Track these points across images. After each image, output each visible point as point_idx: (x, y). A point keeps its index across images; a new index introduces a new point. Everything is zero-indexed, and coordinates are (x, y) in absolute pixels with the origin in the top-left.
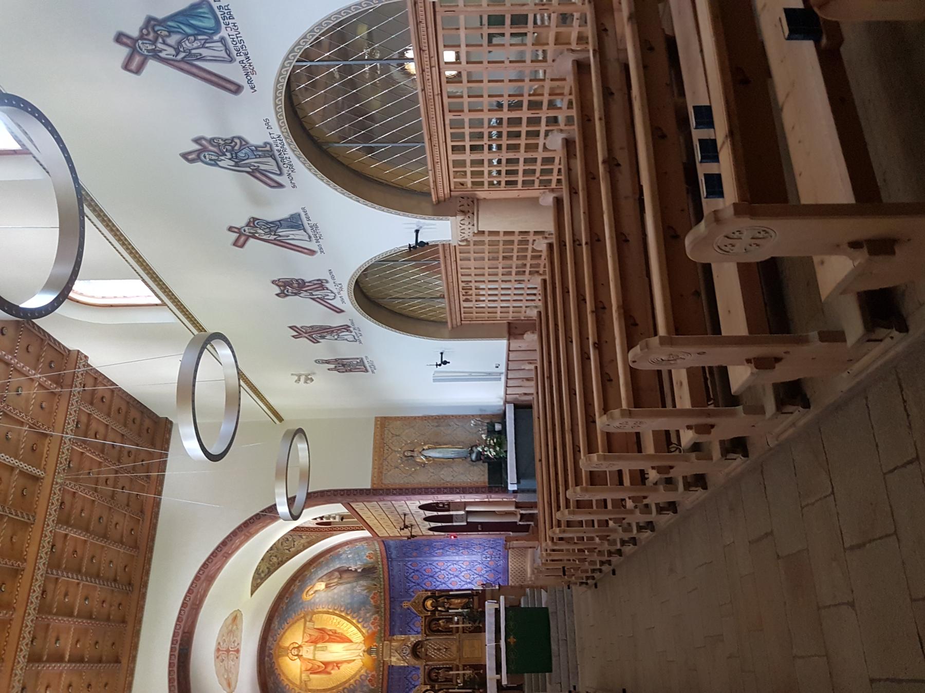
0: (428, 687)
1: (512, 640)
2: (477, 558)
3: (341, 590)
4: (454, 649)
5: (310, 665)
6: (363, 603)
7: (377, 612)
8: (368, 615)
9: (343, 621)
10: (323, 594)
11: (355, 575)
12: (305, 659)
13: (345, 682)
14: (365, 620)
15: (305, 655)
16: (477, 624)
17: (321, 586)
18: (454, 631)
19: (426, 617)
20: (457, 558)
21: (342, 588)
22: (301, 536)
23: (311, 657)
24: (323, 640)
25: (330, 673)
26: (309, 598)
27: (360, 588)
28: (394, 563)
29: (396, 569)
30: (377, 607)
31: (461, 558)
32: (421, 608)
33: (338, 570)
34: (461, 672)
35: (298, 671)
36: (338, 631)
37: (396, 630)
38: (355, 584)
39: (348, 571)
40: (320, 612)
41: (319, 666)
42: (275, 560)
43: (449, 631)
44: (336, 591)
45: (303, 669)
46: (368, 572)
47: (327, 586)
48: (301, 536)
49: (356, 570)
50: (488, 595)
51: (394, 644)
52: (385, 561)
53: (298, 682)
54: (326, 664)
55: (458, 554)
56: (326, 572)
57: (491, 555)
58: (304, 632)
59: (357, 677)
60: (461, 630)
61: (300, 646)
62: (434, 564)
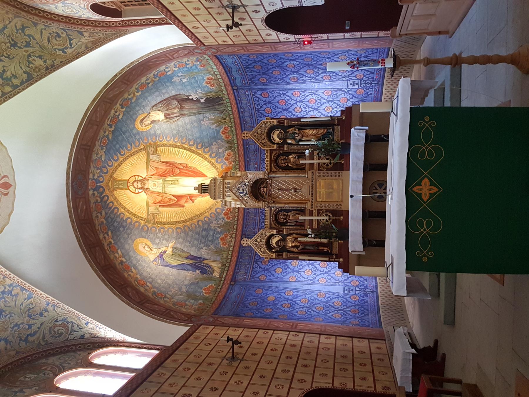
0: (274, 232)
1: (426, 189)
3: (185, 123)
4: (305, 190)
5: (160, 198)
6: (215, 138)
7: (230, 148)
8: (221, 150)
9: (194, 156)
10: (164, 126)
11: (199, 105)
12: (152, 192)
13: (199, 216)
14: (218, 155)
15: (152, 188)
16: (336, 160)
17: (159, 116)
18: (308, 167)
19: (272, 151)
20: (316, 86)
21: (187, 119)
22: (81, 33)
23: (159, 189)
24: (173, 174)
25: (183, 206)
26: (145, 129)
27: (208, 121)
28: (241, 92)
29: (244, 99)
30: (229, 142)
31: (321, 85)
32: (265, 140)
33: (175, 97)
34: (315, 218)
35: (145, 204)
36: (190, 165)
37: (251, 166)
38: (201, 116)
39: (187, 100)
40: (165, 145)
41: (170, 200)
42: (39, 62)
43: (301, 168)
44: (180, 123)
45: (151, 202)
46: (212, 102)
47: (166, 116)
48: (81, 33)
49: (198, 100)
50: (355, 118)
51: (227, 181)
53: (144, 216)
54: (179, 197)
55: (317, 81)
56: (159, 99)
57: (361, 80)
58: (148, 165)
59: (214, 209)
60: (316, 167)
61: (144, 180)
62: (289, 94)
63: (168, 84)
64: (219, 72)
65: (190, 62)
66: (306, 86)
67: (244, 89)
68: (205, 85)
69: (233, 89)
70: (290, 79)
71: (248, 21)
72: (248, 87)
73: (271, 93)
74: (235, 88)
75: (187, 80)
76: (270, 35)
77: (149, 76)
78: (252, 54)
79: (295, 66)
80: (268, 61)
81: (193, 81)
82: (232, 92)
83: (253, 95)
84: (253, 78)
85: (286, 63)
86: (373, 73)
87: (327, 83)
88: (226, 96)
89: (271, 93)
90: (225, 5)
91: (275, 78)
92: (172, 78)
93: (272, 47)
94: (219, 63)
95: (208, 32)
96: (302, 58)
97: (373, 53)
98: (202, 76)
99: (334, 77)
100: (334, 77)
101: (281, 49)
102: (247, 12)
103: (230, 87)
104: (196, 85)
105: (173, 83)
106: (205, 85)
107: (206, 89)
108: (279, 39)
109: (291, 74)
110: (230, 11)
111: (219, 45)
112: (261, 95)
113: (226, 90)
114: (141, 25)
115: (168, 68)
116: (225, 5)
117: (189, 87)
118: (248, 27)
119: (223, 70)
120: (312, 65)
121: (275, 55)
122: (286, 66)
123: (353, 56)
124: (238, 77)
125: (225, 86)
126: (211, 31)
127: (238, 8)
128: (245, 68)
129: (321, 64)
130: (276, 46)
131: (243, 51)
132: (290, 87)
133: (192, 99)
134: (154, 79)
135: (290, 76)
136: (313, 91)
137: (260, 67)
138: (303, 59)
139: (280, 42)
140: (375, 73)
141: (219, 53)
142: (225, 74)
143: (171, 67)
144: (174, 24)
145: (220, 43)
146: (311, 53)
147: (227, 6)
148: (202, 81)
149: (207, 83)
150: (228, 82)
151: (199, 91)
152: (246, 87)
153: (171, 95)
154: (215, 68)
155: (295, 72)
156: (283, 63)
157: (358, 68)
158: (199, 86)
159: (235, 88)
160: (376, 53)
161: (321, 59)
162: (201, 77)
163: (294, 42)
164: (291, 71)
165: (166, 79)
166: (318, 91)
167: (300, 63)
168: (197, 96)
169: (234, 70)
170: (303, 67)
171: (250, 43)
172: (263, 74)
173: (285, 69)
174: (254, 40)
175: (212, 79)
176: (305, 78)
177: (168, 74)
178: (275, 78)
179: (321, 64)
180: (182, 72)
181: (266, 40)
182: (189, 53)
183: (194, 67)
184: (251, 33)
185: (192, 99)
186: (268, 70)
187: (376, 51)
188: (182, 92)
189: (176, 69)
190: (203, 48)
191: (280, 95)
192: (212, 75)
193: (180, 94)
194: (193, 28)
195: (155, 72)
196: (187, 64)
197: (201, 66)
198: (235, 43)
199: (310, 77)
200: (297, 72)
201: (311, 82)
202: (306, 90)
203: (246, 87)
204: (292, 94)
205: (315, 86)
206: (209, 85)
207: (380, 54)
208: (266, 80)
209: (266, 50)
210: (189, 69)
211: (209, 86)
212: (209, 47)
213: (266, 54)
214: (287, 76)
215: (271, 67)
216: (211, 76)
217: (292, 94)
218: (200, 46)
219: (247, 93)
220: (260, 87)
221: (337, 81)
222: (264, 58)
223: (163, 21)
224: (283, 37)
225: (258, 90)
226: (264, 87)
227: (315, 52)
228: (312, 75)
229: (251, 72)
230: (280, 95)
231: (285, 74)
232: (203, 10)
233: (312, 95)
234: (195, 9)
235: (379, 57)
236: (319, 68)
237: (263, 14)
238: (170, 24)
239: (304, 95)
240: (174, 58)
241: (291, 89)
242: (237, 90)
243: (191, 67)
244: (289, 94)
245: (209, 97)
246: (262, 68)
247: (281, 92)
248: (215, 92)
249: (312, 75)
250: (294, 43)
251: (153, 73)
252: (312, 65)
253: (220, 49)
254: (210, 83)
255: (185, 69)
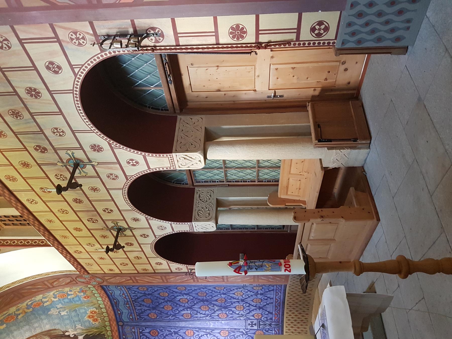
2: (239, 324)
20: (212, 325)
28: (127, 329)
52: (114, 324)
55: (212, 319)
57: (259, 320)
62: (181, 332)
63: (43, 317)
64: (105, 305)
65: (72, 293)
66: (200, 324)
67: (131, 326)
68: (87, 319)
69: (118, 325)
70: (182, 316)
71: (136, 247)
72: (135, 324)
73: (162, 331)
74: (121, 323)
75: (67, 312)
76: (161, 264)
77: (20, 305)
78: (142, 286)
79: (188, 301)
80: (159, 294)
81: (73, 314)
82: (116, 328)
83: (140, 333)
84: (142, 313)
85: (178, 298)
86: (272, 313)
87: (223, 322)
88: (109, 333)
89: (162, 331)
90: (110, 227)
91: (167, 314)
92: (49, 310)
93: (163, 278)
94: (105, 295)
95: (92, 258)
96: (196, 292)
97: (269, 291)
98: (85, 309)
99: (231, 316)
100: (231, 316)
101: (173, 281)
102: (134, 236)
103: (115, 323)
104: (76, 319)
105: (49, 316)
106: (87, 319)
107: (87, 324)
108: (170, 269)
109: (184, 310)
110: (115, 233)
111: (105, 273)
112: (149, 333)
113: (111, 326)
114: (17, 245)
115: (45, 298)
116: (110, 227)
117: (68, 322)
118: (136, 254)
119: (109, 303)
120: (207, 301)
121: (167, 288)
122: (179, 301)
123: (249, 292)
124: (125, 312)
125: (110, 321)
126: (95, 256)
127: (125, 231)
128: (134, 302)
129: (216, 300)
130: (167, 277)
131: (131, 281)
132: (183, 324)
133: (69, 336)
134: (26, 311)
135: (183, 312)
136: (208, 331)
137: (150, 301)
138: (197, 294)
139: (172, 272)
140: (274, 313)
141: (105, 283)
142: (111, 307)
143: (50, 296)
144: (53, 246)
145: (107, 271)
146: (205, 287)
147: (112, 228)
148: (84, 315)
149: (89, 317)
150: (114, 317)
151: (79, 326)
152: (133, 324)
153: (44, 330)
154: (100, 300)
155: (188, 308)
156: (175, 297)
157: (246, 273)
158: (80, 321)
159: (121, 323)
160: (273, 290)
161: (216, 294)
162: (83, 311)
163: (186, 273)
164: (184, 306)
165: (42, 310)
166: (213, 330)
167: (194, 297)
168: (75, 333)
169: (121, 303)
170: (197, 303)
171: (138, 273)
172: (154, 308)
173: (177, 304)
174: (144, 270)
175: (95, 312)
176: (199, 315)
177: (45, 304)
178: (167, 314)
179: (216, 300)
180: (62, 304)
181: (157, 270)
182: (71, 281)
183: (77, 299)
184: (140, 261)
185: (69, 336)
186: (159, 304)
187: (272, 288)
188: (58, 327)
189: (55, 300)
190: (87, 276)
191: (171, 334)
192: (96, 309)
193: (55, 329)
194: (75, 252)
195: (28, 302)
196: (69, 295)
197: (85, 297)
198: (123, 272)
199: (205, 314)
200: (190, 308)
201: (206, 320)
202: (200, 329)
203: (133, 324)
204: (185, 333)
205: (210, 325)
206: (91, 320)
207: (276, 292)
208: (156, 316)
209: (157, 281)
210: (71, 301)
211: (91, 321)
212: (94, 276)
213: (157, 286)
214: (179, 312)
215: (163, 301)
216: (95, 309)
217: (185, 333)
218: (84, 274)
219: (133, 330)
220: (149, 324)
221: (234, 320)
222: (155, 291)
223: (42, 242)
224: (175, 266)
225: (146, 327)
226: (153, 324)
227: (210, 286)
228: (207, 312)
229: (140, 306)
230: (171, 334)
231: (177, 309)
232: (85, 232)
233: (207, 335)
234: (76, 229)
235: (276, 295)
236: (214, 305)
237: (152, 240)
238: (49, 246)
239: (198, 335)
240: (54, 287)
241: (184, 327)
242: (122, 326)
243: (73, 298)
244: (181, 332)
245: (89, 333)
246: (152, 302)
247: (172, 331)
248: (96, 328)
249: (207, 312)
250: (186, 273)
251: (26, 303)
252: (207, 301)
253: (106, 278)
254: (93, 317)
255: (66, 300)
